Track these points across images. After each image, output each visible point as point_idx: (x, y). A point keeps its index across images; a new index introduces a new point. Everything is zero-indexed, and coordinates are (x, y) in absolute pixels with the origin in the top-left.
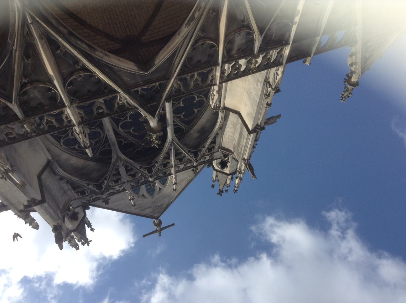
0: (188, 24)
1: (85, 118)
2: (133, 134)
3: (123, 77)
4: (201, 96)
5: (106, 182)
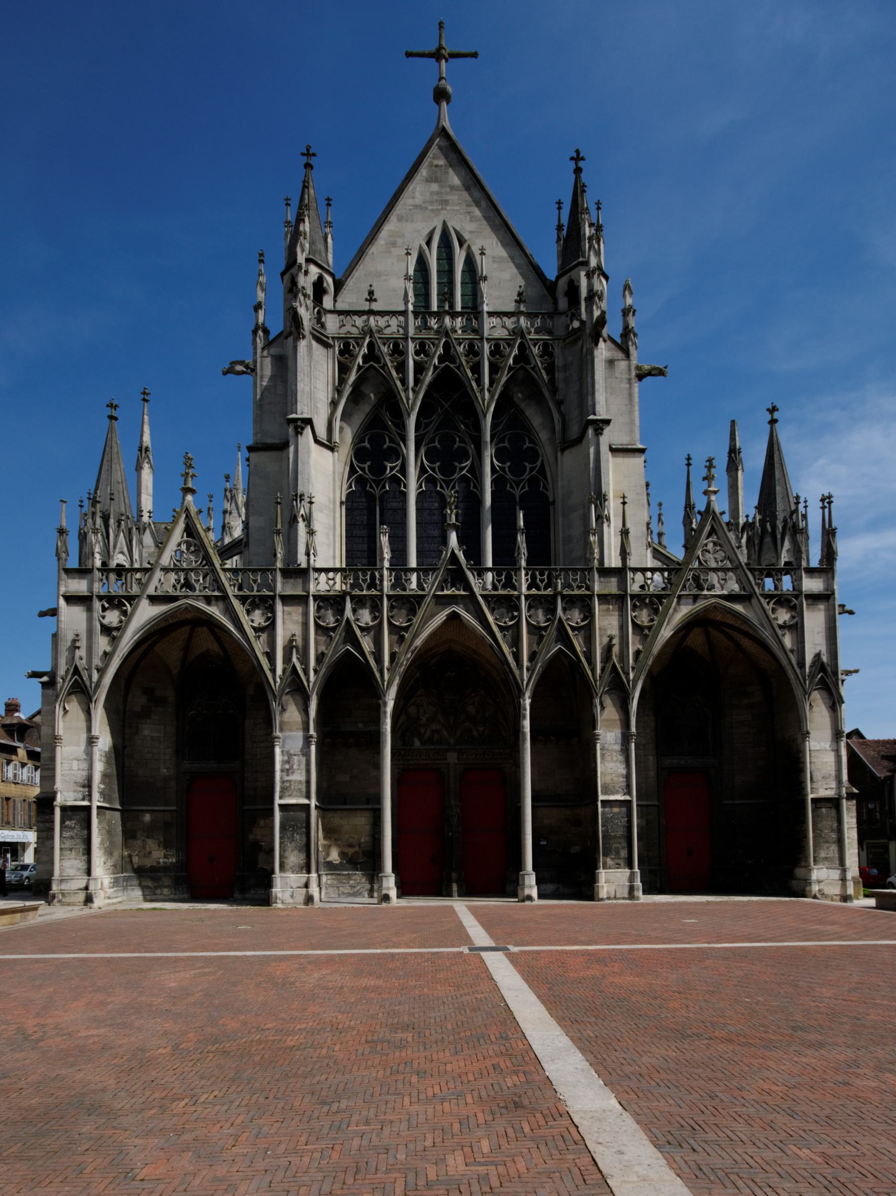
0: (416, 648)
5: (511, 361)
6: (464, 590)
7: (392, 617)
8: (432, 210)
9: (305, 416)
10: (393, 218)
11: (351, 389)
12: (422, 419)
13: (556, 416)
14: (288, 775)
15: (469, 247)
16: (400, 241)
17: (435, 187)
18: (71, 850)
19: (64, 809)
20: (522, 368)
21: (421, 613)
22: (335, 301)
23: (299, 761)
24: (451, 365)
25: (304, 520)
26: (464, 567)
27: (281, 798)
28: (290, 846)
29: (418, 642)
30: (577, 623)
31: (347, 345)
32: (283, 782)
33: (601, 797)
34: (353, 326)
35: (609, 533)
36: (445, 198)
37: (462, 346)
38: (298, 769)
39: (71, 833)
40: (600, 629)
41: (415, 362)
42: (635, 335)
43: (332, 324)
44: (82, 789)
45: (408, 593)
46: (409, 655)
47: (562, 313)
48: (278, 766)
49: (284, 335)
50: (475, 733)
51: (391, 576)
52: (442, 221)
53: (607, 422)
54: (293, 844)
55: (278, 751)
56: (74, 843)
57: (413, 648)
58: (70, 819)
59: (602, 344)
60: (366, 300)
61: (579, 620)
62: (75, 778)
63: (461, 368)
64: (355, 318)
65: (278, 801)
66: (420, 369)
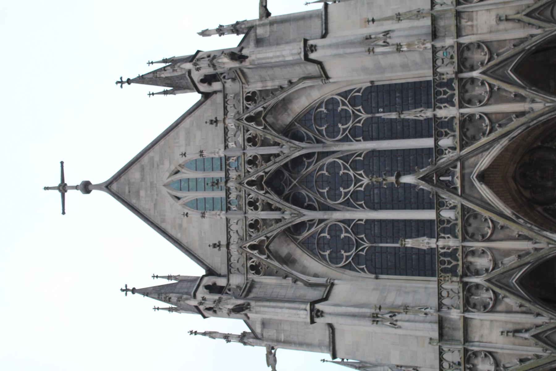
0: (514, 214)
1: (439, 121)
2: (317, 172)
3: (473, 159)
4: (350, 259)
5: (260, 128)
6: (455, 167)
7: (483, 236)
8: (157, 195)
9: (308, 307)
10: (163, 226)
11: (285, 266)
12: (306, 204)
13: (301, 86)
15: (180, 165)
16: (178, 221)
17: (142, 193)
20: (264, 118)
22: (219, 275)
24: (265, 179)
25: (395, 315)
26: (434, 168)
29: (508, 212)
30: (485, 55)
31: (252, 268)
34: (238, 262)
35: (400, 30)
36: (149, 184)
37: (250, 170)
40: (491, 32)
41: (262, 210)
42: (238, 23)
43: (237, 280)
45: (459, 222)
46: (521, 221)
47: (224, 86)
49: (246, 319)
51: (444, 238)
52: (163, 187)
53: (306, 41)
57: (514, 217)
59: (245, 52)
60: (219, 250)
61: (483, 54)
63: (267, 170)
64: (232, 259)
66: (268, 207)
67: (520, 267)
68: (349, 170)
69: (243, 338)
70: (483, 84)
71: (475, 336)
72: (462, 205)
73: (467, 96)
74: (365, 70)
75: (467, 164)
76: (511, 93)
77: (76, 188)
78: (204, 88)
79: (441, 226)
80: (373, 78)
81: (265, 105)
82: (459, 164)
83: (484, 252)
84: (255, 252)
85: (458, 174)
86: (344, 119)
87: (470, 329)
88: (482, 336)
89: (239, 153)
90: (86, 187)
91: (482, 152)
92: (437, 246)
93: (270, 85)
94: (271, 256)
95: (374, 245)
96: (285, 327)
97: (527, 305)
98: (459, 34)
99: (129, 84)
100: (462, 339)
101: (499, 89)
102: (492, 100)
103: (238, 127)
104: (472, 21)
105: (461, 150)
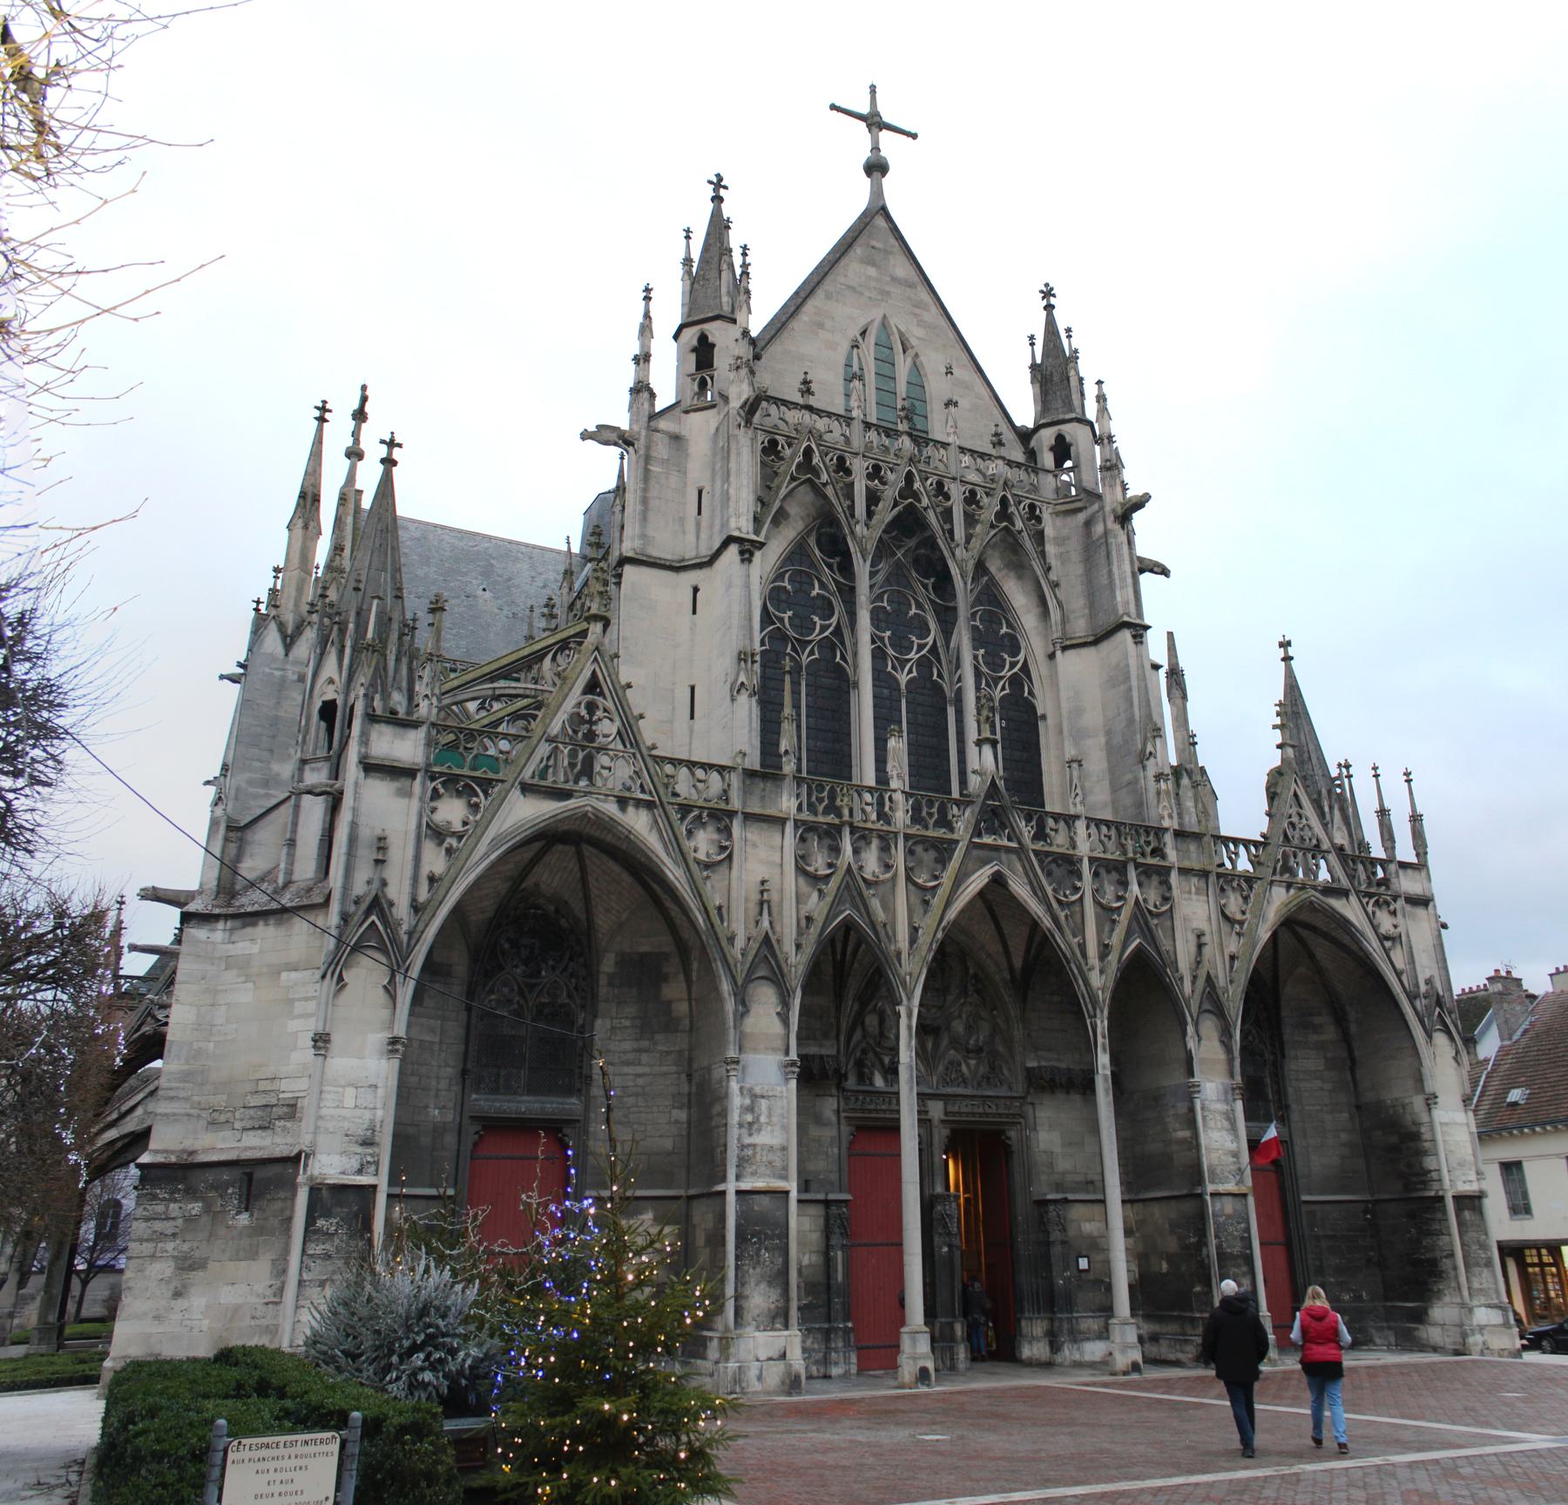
6: (1010, 839)
10: (820, 293)
14: (750, 1135)
17: (872, 271)
18: (322, 1284)
19: (315, 1190)
21: (954, 864)
23: (770, 1109)
27: (738, 1178)
28: (753, 1274)
29: (952, 914)
32: (743, 1147)
33: (1210, 1188)
37: (929, 482)
38: (768, 1124)
39: (327, 1246)
44: (359, 1149)
48: (734, 1117)
50: (964, 1068)
54: (758, 1270)
55: (734, 1086)
56: (330, 1268)
58: (327, 1215)
62: (346, 1125)
65: (731, 1187)
67: (873, 925)
68: (917, 653)
69: (641, 390)
70: (1119, 898)
71: (755, 834)
72: (957, 842)
73: (1102, 871)
74: (1078, 711)
75: (1014, 857)
76: (1110, 938)
77: (876, 148)
78: (1047, 436)
79: (924, 802)
80: (1050, 720)
81: (1025, 534)
82: (1014, 845)
83: (888, 867)
84: (799, 459)
85: (1000, 842)
86: (990, 660)
87: (765, 826)
88: (754, 845)
89: (953, 471)
90: (876, 168)
91: (1031, 883)
92: (895, 791)
93: (1050, 549)
94: (794, 484)
95: (804, 672)
96: (674, 480)
97: (814, 931)
98: (1184, 872)
99: (1045, 308)
100: (748, 810)
101: (1114, 921)
102: (1099, 910)
103: (992, 480)
104: (1196, 893)
105: (1033, 850)
